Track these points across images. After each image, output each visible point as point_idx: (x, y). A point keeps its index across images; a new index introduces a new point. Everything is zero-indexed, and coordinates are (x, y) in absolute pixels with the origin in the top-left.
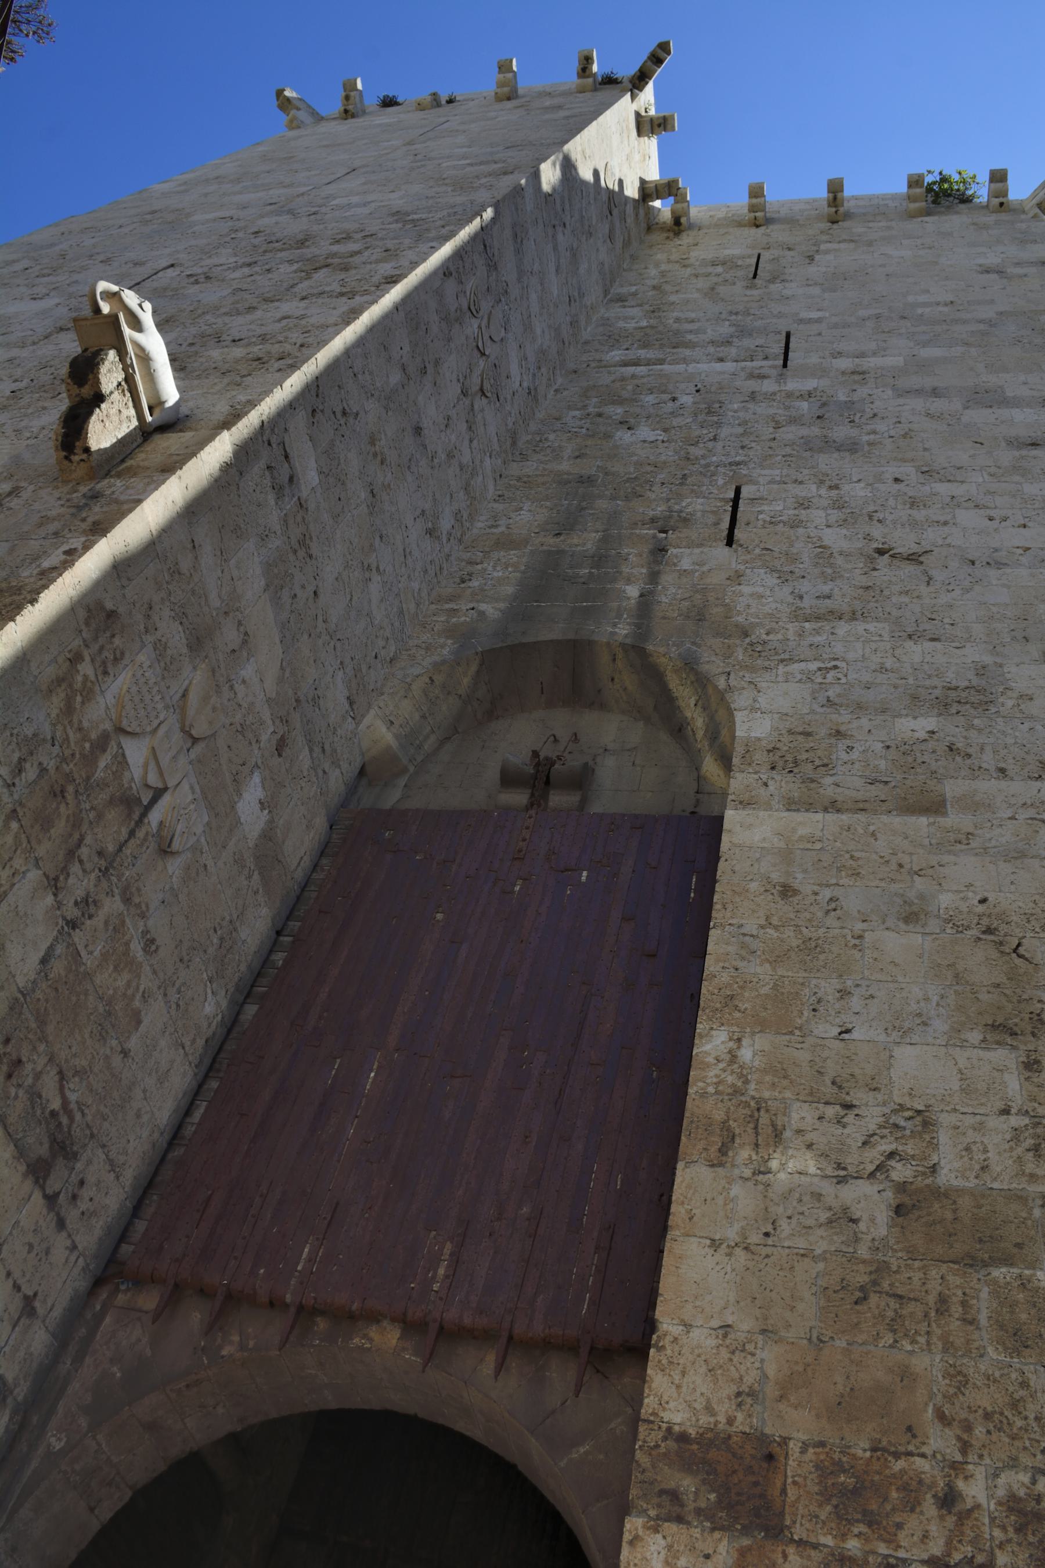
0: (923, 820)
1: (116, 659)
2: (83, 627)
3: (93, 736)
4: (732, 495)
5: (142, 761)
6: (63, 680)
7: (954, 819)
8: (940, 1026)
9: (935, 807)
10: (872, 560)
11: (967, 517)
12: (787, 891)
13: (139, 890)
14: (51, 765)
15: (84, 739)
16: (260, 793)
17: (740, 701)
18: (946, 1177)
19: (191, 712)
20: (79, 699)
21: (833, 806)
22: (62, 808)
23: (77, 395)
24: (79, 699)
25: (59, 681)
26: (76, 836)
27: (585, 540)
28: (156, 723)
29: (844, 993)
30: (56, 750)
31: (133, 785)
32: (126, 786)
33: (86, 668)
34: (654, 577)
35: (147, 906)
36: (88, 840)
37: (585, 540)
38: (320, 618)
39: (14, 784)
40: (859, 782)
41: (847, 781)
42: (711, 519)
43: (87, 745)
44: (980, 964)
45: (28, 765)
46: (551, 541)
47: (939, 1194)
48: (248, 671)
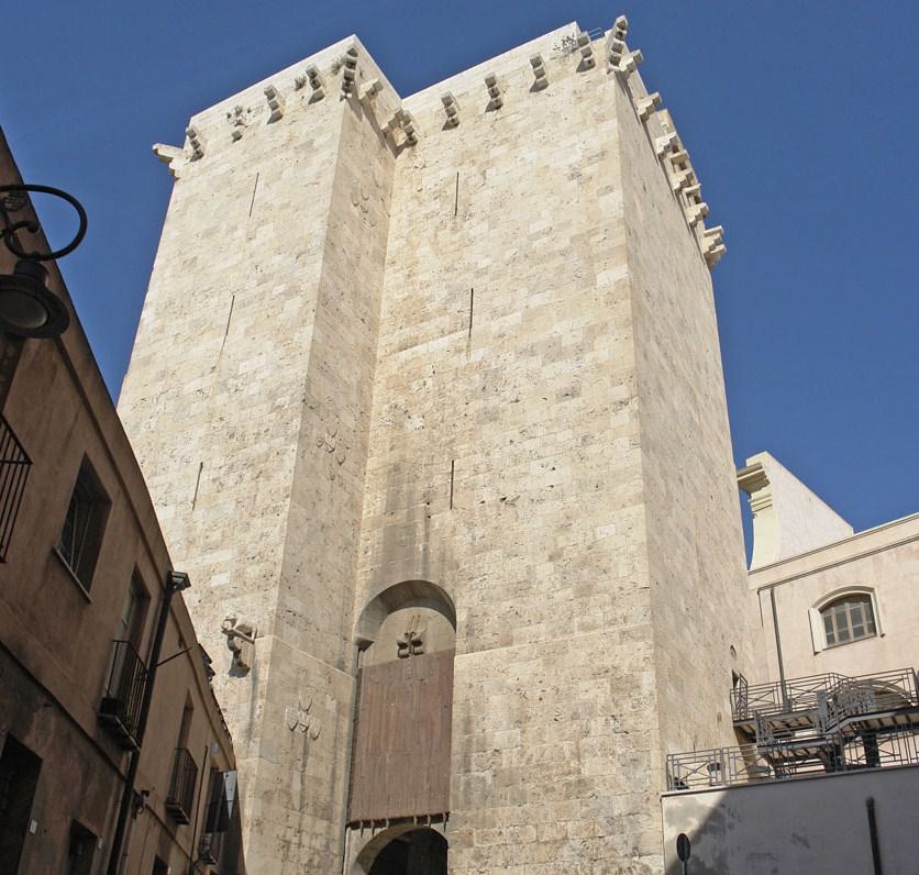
0: (505, 649)
4: (450, 470)
7: (515, 647)
8: (505, 723)
9: (509, 643)
10: (499, 507)
11: (535, 467)
12: (471, 686)
17: (458, 605)
18: (504, 766)
21: (483, 649)
27: (402, 515)
29: (484, 719)
34: (427, 535)
37: (402, 515)
40: (489, 636)
41: (487, 637)
42: (444, 491)
44: (515, 703)
46: (391, 518)
47: (502, 771)
48: (312, 677)
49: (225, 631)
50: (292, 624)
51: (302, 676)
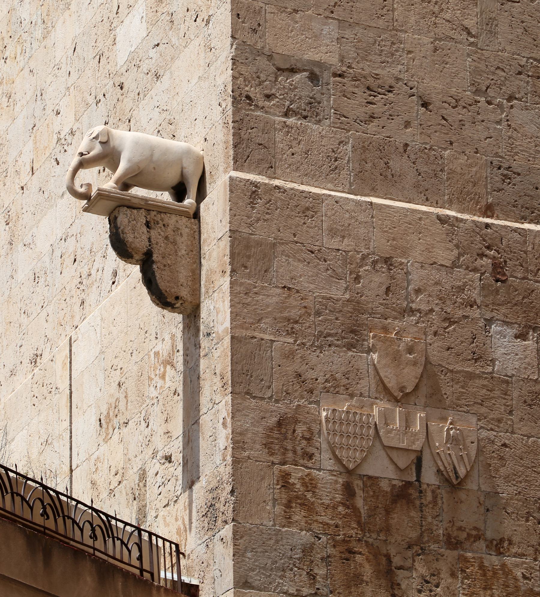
1: (309, 440)
2: (271, 459)
3: (339, 498)
5: (386, 462)
6: (290, 501)
13: (460, 529)
14: (330, 550)
15: (335, 508)
16: (510, 332)
19: (391, 384)
20: (309, 495)
22: (358, 558)
23: (137, 261)
24: (309, 495)
25: (288, 506)
26: (384, 560)
28: (372, 432)
30: (324, 538)
31: (394, 482)
32: (389, 489)
33: (297, 473)
35: (475, 528)
36: (393, 551)
38: (448, 111)
39: (318, 589)
43: (340, 509)
45: (316, 571)
49: (92, 201)
50: (311, 111)
51: (374, 282)
